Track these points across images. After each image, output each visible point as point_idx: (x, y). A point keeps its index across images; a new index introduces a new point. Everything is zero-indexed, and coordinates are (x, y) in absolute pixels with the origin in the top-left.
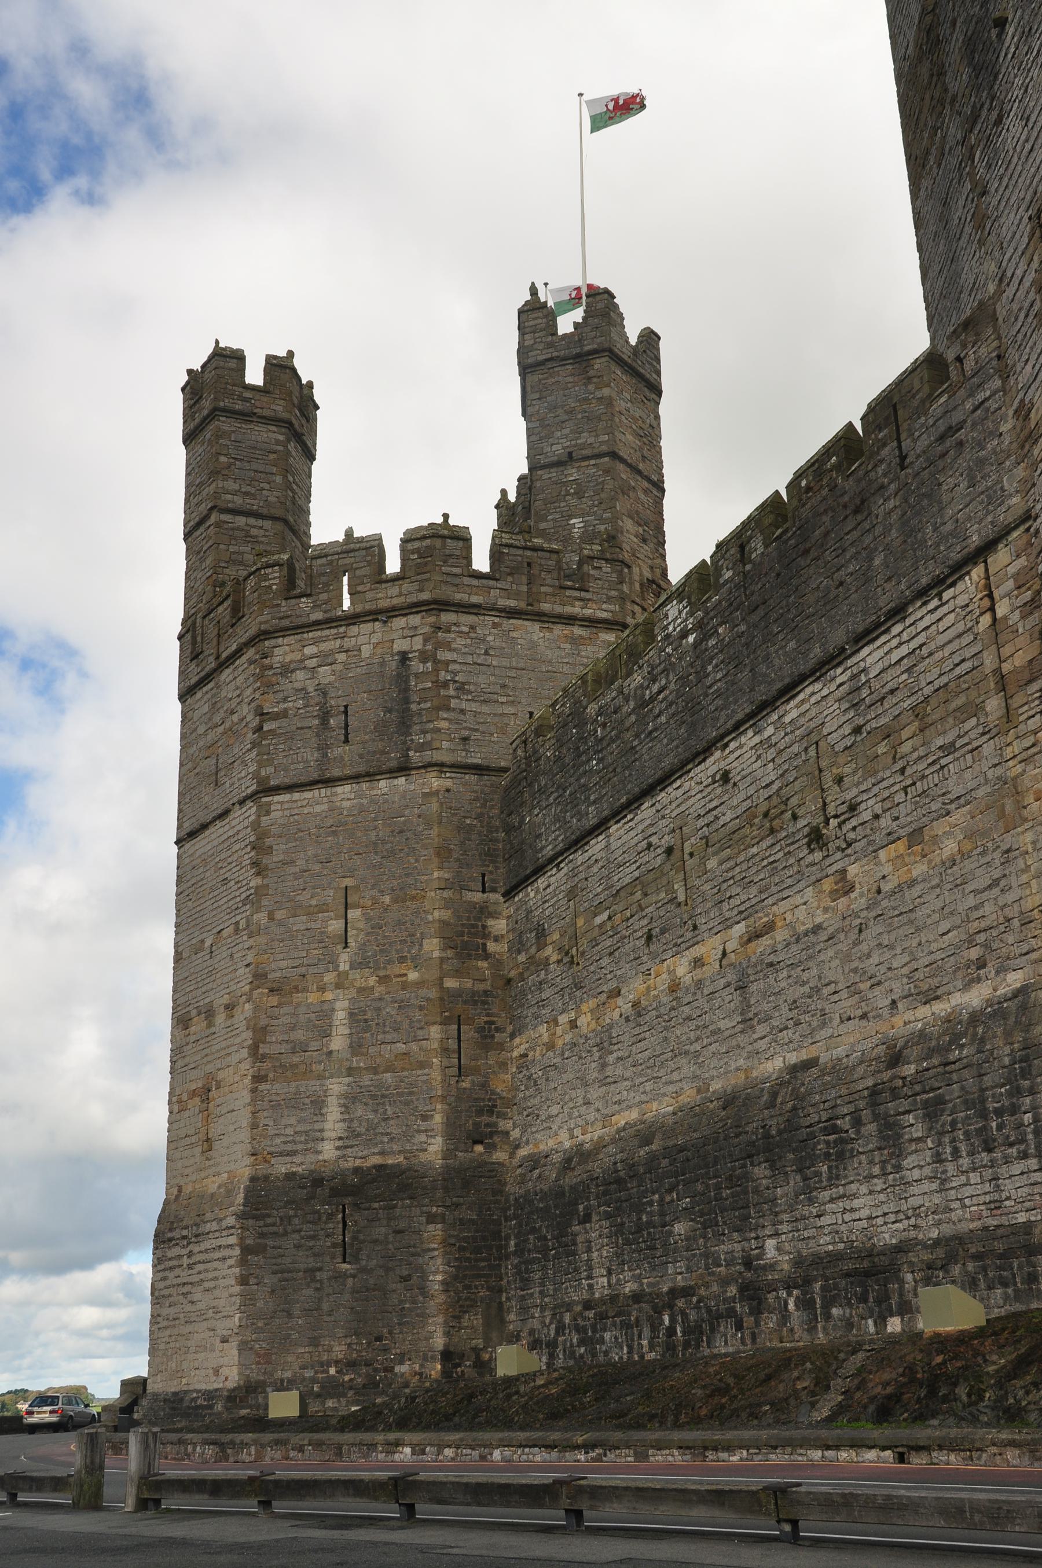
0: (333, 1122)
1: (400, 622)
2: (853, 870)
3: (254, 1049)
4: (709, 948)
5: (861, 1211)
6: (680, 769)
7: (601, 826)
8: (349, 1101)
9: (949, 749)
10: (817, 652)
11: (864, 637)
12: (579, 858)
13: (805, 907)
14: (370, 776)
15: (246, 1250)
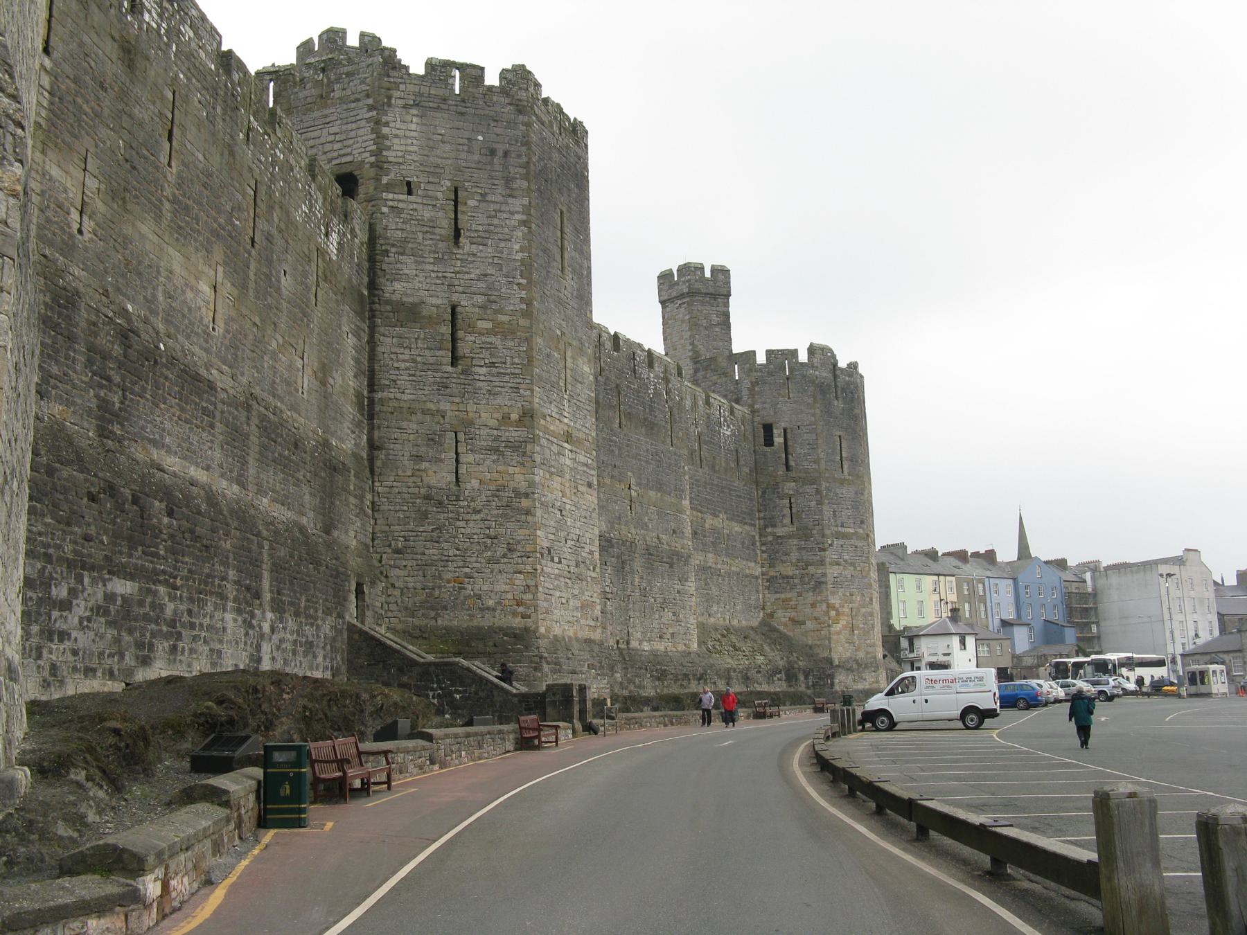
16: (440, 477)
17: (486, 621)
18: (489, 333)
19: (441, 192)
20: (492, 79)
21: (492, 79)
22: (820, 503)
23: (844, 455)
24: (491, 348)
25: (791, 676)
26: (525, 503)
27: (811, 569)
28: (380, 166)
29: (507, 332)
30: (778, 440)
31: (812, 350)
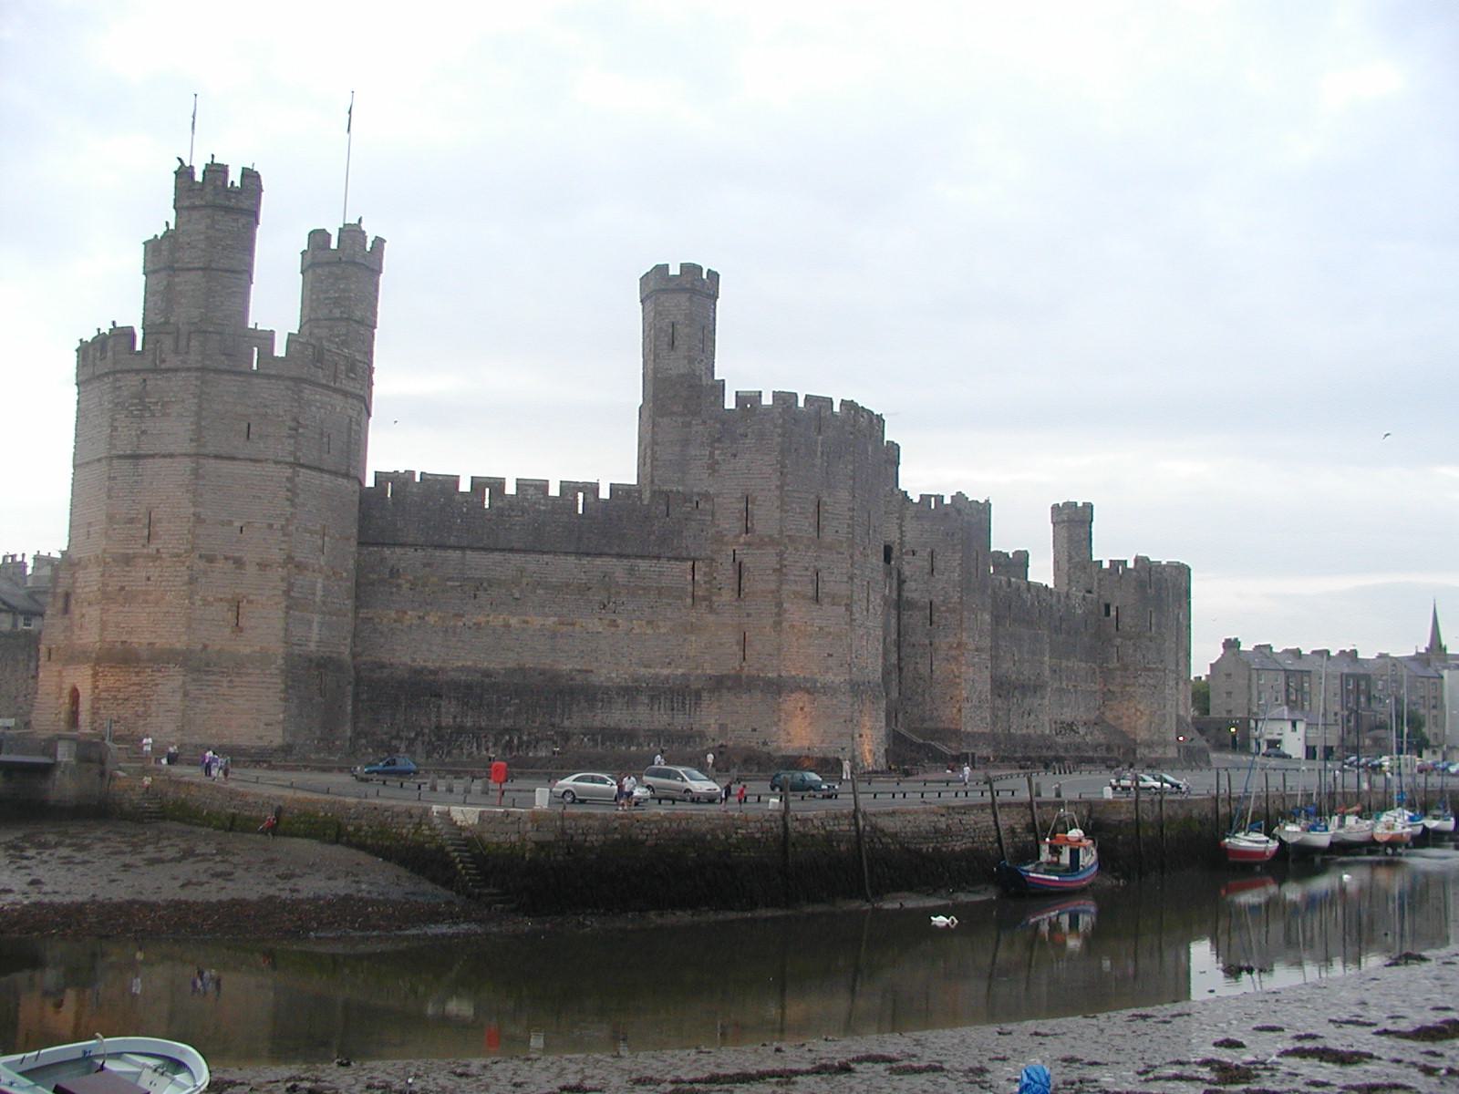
0: (315, 635)
1: (350, 401)
2: (620, 621)
3: (287, 593)
4: (537, 621)
5: (618, 717)
6: (525, 551)
7: (463, 548)
8: (322, 624)
9: (670, 605)
10: (616, 550)
11: (642, 557)
12: (437, 553)
13: (595, 625)
14: (336, 473)
15: (288, 687)
16: (924, 670)
17: (941, 725)
18: (945, 612)
19: (926, 554)
20: (947, 501)
21: (947, 501)
22: (1135, 651)
23: (1153, 621)
24: (946, 619)
25: (1109, 749)
26: (958, 680)
27: (1128, 689)
28: (902, 544)
29: (953, 611)
30: (1113, 613)
31: (1137, 560)
